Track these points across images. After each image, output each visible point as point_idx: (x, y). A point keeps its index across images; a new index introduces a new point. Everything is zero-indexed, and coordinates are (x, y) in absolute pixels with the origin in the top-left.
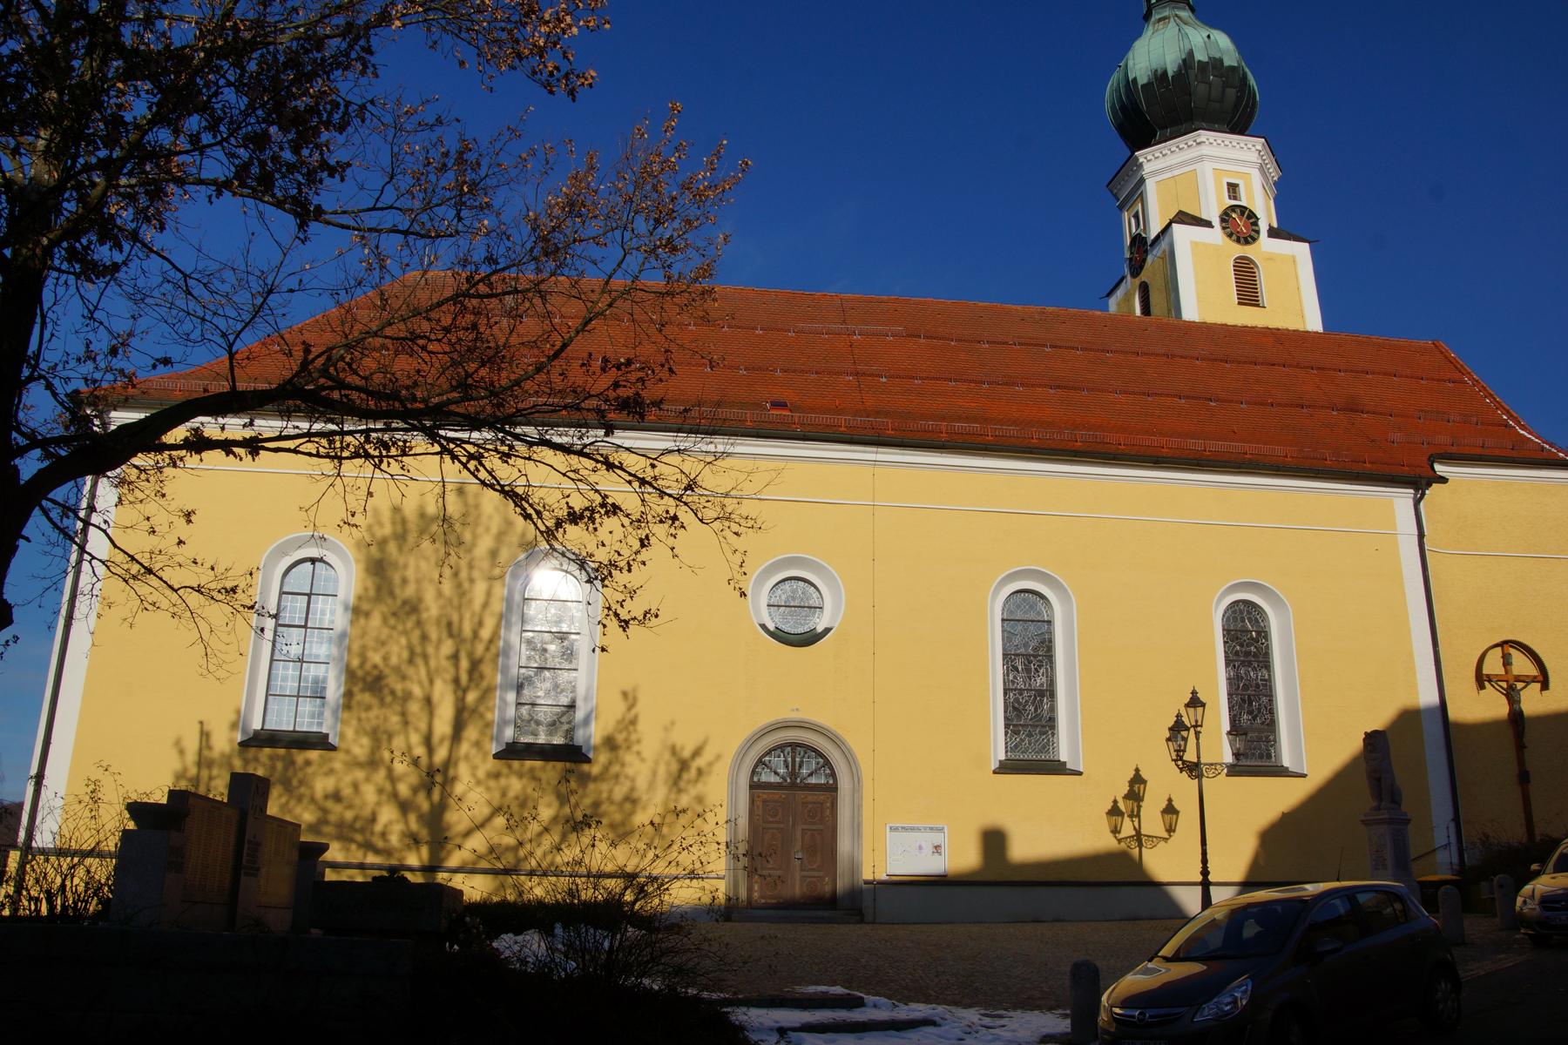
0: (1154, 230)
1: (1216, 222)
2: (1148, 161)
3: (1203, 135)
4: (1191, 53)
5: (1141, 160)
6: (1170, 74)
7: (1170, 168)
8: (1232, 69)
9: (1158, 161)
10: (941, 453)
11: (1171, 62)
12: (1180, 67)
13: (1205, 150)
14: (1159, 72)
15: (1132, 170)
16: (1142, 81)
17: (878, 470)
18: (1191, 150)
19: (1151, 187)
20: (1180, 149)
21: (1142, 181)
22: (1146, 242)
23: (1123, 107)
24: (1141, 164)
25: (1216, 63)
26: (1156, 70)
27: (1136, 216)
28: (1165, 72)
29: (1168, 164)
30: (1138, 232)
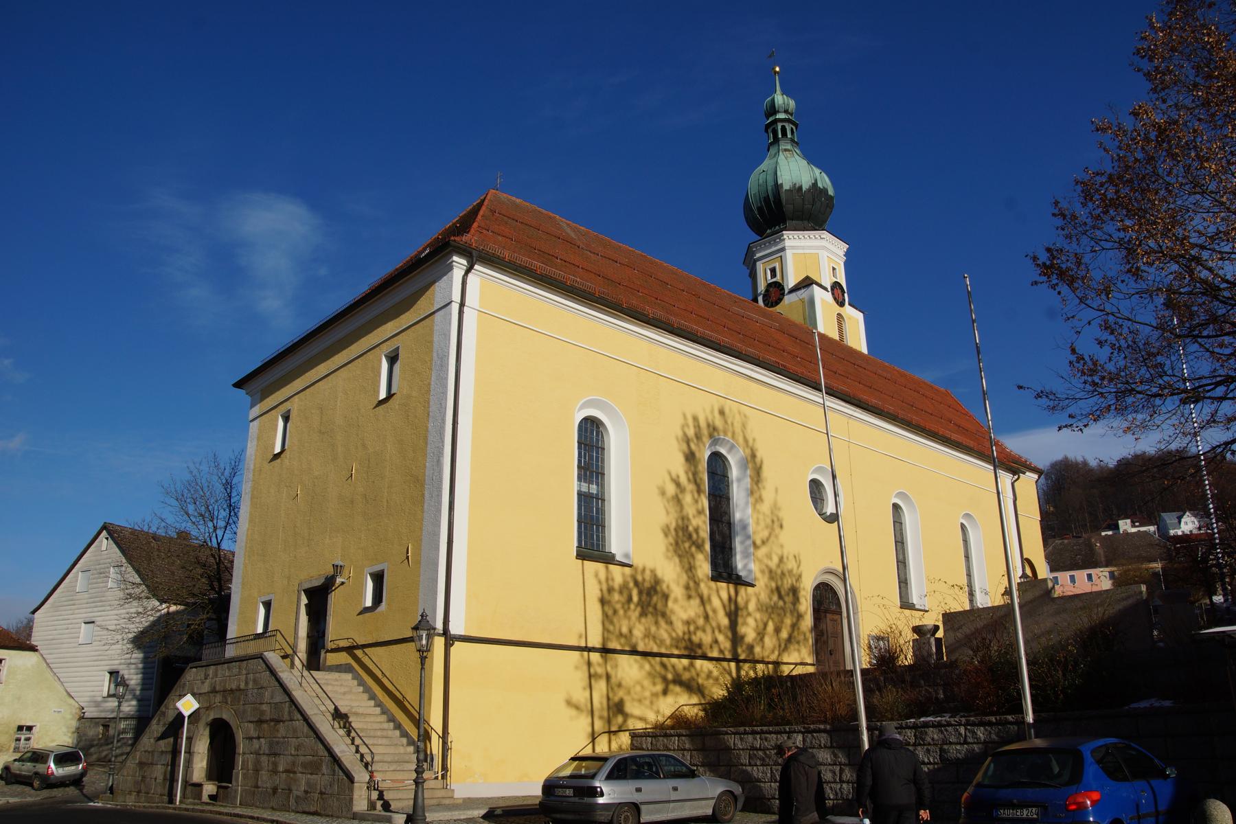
0: (791, 282)
1: (829, 289)
2: (789, 239)
3: (825, 234)
4: (816, 180)
5: (785, 237)
6: (804, 189)
7: (803, 248)
8: (831, 196)
9: (795, 241)
10: (876, 417)
11: (806, 184)
12: (810, 186)
13: (823, 243)
14: (797, 185)
15: (775, 241)
16: (786, 187)
17: (850, 421)
18: (816, 241)
19: (789, 254)
20: (821, 238)
21: (783, 249)
22: (783, 289)
23: (767, 199)
24: (784, 239)
25: (825, 191)
26: (795, 184)
27: (773, 271)
28: (800, 188)
29: (799, 244)
30: (774, 280)
